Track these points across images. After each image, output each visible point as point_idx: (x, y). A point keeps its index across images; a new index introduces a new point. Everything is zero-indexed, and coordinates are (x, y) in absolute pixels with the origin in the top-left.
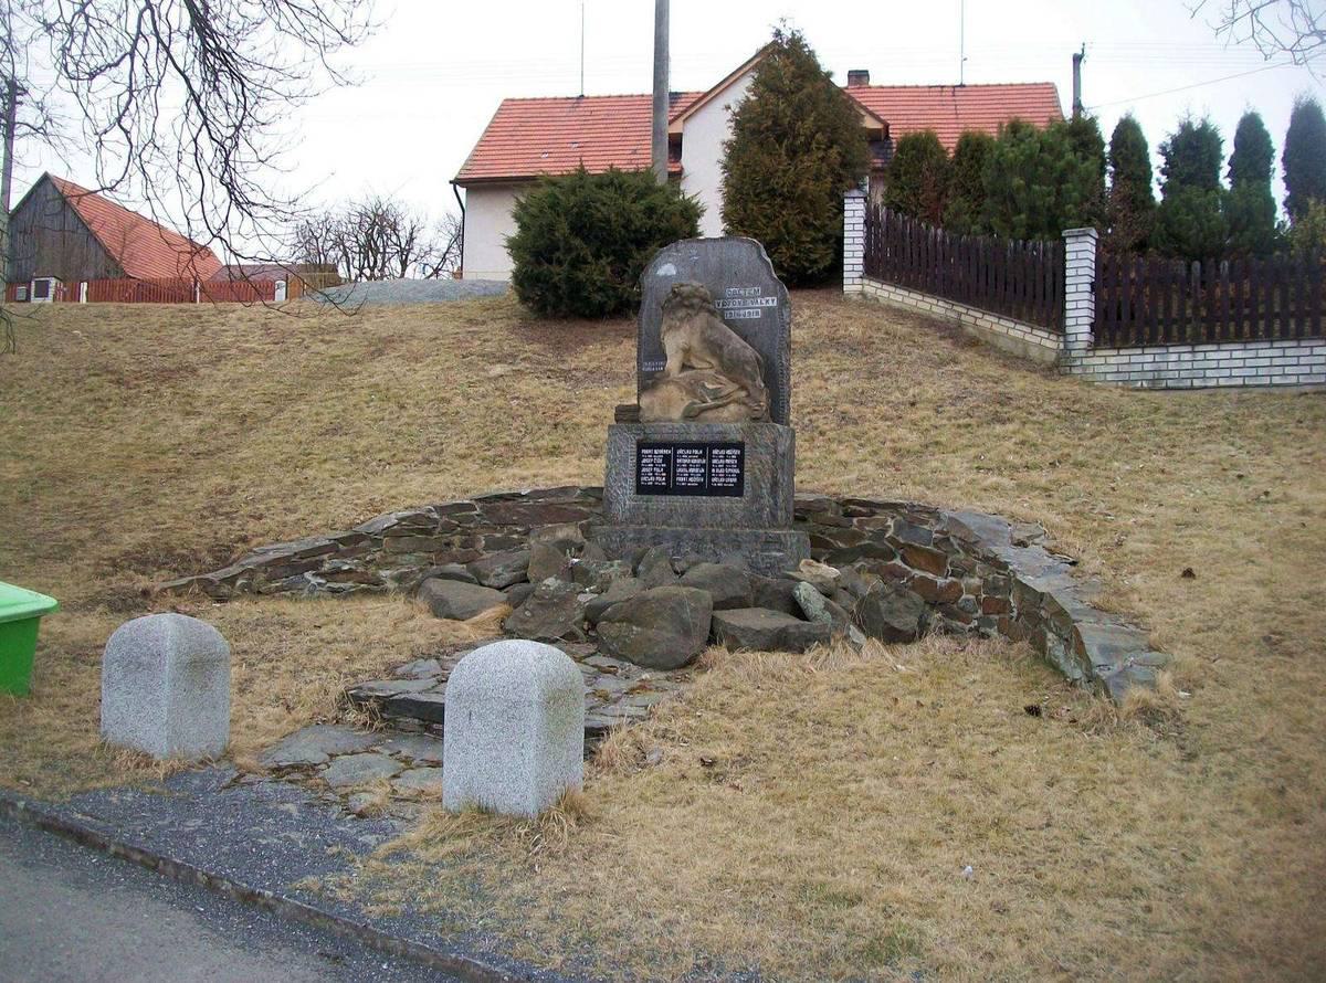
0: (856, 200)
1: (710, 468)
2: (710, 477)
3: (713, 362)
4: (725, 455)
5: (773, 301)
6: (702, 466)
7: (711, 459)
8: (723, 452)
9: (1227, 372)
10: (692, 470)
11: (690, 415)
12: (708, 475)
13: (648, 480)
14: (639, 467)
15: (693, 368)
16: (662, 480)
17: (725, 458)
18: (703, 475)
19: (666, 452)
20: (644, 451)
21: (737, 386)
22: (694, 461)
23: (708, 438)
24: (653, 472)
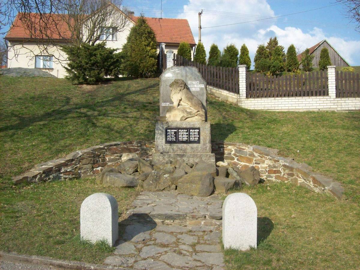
2: (190, 138)
6: (187, 135)
8: (193, 130)
10: (183, 136)
13: (169, 139)
16: (174, 139)
17: (194, 132)
18: (187, 137)
22: (184, 133)
23: (188, 126)
24: (171, 137)
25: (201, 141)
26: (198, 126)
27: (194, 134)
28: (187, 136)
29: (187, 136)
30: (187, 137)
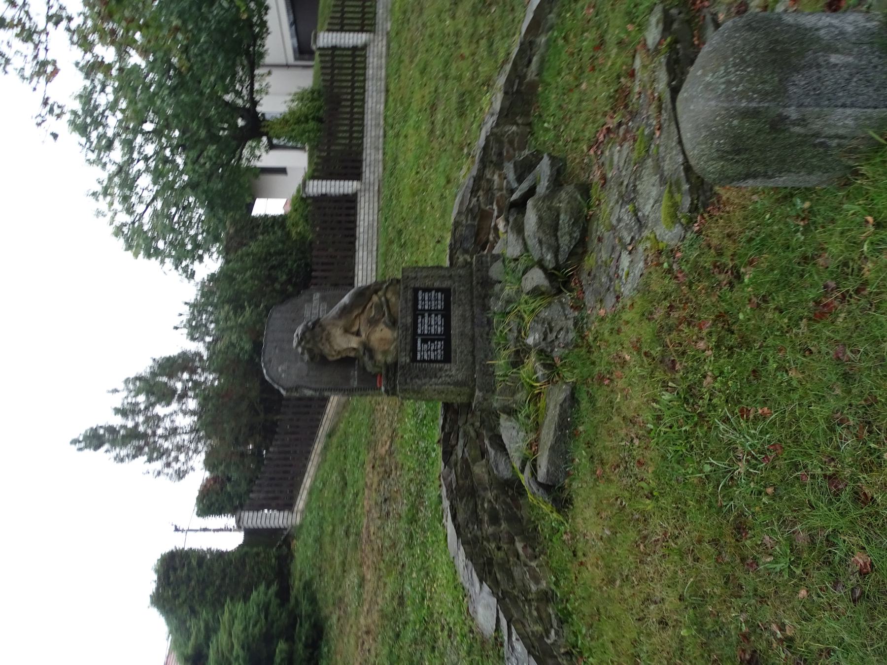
2: (437, 310)
3: (356, 313)
6: (430, 315)
7: (424, 310)
8: (420, 302)
9: (369, 272)
10: (433, 323)
11: (393, 323)
12: (436, 312)
16: (440, 344)
18: (436, 315)
20: (419, 357)
22: (426, 321)
23: (410, 311)
25: (446, 284)
28: (433, 316)
29: (433, 316)
30: (436, 315)
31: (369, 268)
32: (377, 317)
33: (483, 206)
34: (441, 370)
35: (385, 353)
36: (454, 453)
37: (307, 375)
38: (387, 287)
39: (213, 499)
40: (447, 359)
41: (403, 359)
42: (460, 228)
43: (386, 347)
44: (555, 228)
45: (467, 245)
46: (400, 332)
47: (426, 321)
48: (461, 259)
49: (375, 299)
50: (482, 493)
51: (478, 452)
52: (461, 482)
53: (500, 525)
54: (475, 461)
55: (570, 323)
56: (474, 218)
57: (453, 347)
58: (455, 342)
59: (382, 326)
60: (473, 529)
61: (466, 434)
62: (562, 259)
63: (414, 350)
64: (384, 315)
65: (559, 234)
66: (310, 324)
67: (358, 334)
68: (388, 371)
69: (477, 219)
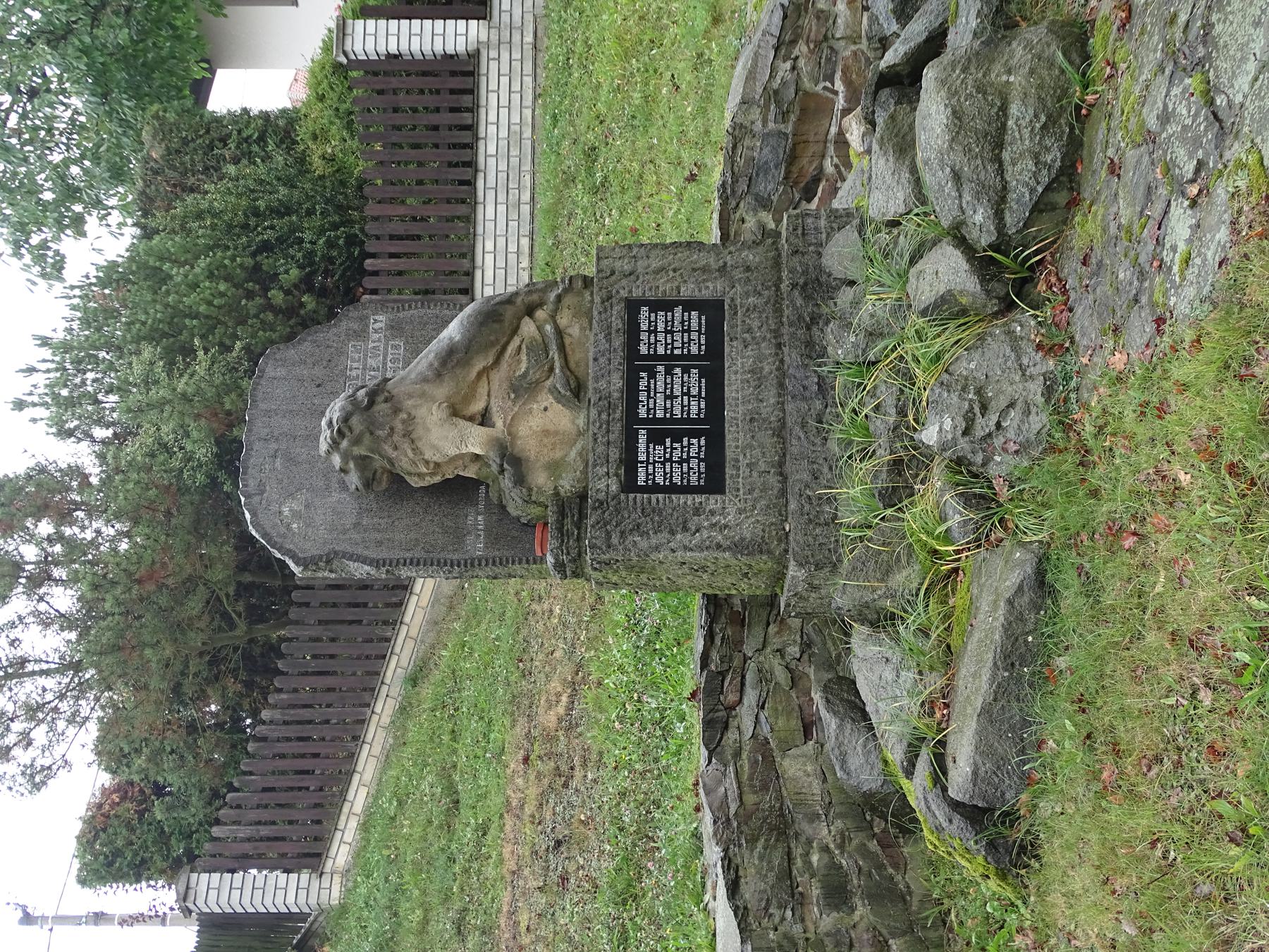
0: (193, 884)
1: (672, 357)
2: (689, 357)
3: (479, 365)
4: (650, 332)
5: (376, 321)
6: (669, 371)
7: (656, 357)
8: (644, 336)
9: (512, 258)
10: (677, 392)
11: (576, 391)
13: (696, 472)
14: (672, 489)
15: (487, 410)
16: (696, 446)
17: (655, 332)
18: (686, 370)
19: (642, 439)
21: (527, 319)
22: (660, 385)
23: (618, 358)
25: (711, 289)
26: (617, 315)
27: (666, 332)
28: (678, 371)
29: (678, 371)
30: (686, 370)
31: (513, 248)
32: (534, 375)
33: (807, 84)
34: (697, 511)
35: (554, 468)
36: (733, 723)
37: (356, 525)
38: (559, 298)
39: (120, 843)
40: (714, 482)
41: (601, 485)
42: (747, 142)
43: (558, 454)
44: (997, 140)
45: (769, 185)
46: (594, 412)
47: (660, 385)
48: (751, 223)
49: (528, 328)
50: (807, 828)
51: (796, 723)
52: (750, 799)
53: (853, 909)
54: (786, 747)
55: (1035, 390)
56: (784, 116)
57: (729, 454)
58: (734, 439)
59: (546, 399)
60: (783, 919)
61: (764, 677)
62: (1012, 220)
63: (630, 462)
64: (551, 369)
65: (1006, 156)
66: (362, 392)
67: (484, 419)
68: (562, 514)
69: (793, 118)
